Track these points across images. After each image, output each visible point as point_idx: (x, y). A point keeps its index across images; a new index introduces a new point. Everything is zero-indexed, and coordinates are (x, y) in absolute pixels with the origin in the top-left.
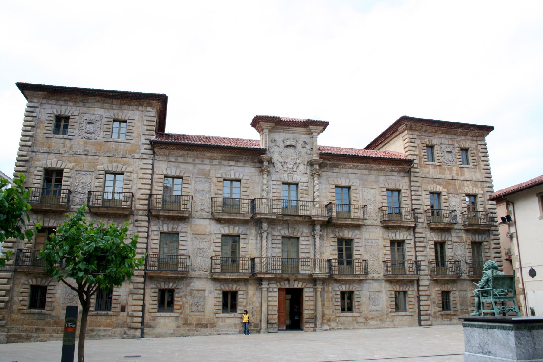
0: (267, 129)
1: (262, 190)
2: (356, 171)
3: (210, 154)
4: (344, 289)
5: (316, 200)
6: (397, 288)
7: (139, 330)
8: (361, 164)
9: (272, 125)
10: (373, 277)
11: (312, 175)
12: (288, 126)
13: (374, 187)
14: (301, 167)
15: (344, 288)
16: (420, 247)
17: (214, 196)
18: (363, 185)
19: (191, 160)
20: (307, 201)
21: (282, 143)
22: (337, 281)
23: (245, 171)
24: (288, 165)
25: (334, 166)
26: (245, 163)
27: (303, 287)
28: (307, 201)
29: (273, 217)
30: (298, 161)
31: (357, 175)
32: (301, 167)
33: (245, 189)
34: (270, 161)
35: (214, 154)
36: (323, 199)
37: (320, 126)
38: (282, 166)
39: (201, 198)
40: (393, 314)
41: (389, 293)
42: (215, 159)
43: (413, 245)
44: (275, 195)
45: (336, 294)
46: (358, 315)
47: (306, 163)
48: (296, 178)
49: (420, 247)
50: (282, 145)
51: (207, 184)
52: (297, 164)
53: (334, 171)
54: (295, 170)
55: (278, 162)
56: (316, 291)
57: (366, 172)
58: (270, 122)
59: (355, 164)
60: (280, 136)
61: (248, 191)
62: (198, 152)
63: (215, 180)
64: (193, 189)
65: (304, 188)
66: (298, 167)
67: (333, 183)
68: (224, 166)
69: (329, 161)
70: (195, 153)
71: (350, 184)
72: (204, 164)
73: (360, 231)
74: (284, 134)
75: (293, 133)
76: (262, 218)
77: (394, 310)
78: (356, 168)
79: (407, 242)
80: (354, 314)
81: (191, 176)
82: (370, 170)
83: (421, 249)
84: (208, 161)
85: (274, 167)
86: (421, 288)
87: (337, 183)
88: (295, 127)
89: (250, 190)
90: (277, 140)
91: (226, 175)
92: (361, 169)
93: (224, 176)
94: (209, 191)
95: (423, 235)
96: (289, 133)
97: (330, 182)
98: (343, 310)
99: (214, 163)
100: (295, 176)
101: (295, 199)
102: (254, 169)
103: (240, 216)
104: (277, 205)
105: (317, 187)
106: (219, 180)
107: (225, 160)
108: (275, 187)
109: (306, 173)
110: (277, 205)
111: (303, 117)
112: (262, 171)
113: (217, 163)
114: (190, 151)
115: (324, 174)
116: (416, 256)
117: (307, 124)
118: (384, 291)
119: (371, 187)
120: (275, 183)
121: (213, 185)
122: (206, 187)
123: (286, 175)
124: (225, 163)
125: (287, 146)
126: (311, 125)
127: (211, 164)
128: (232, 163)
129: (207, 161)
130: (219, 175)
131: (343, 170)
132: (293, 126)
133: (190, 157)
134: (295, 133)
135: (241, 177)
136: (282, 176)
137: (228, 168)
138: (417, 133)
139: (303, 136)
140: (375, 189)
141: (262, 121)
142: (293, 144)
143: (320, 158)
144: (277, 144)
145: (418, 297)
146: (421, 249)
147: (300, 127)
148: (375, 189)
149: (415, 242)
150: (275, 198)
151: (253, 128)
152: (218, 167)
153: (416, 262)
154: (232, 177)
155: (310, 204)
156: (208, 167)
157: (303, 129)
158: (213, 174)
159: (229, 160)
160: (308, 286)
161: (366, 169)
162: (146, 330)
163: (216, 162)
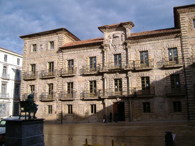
4: (144, 102)
6: (174, 100)
7: (61, 121)
10: (160, 95)
15: (144, 101)
16: (188, 77)
22: (140, 98)
27: (124, 101)
40: (172, 113)
41: (169, 102)
43: (183, 76)
45: (140, 104)
46: (152, 114)
49: (188, 77)
56: (129, 103)
73: (152, 71)
77: (173, 111)
79: (181, 75)
80: (150, 114)
83: (188, 78)
86: (189, 99)
95: (190, 70)
98: (145, 111)
116: (186, 82)
118: (166, 102)
138: (186, 14)
145: (188, 104)
146: (188, 78)
149: (185, 74)
153: (186, 85)
158: (84, 56)
160: (126, 101)
162: (63, 120)
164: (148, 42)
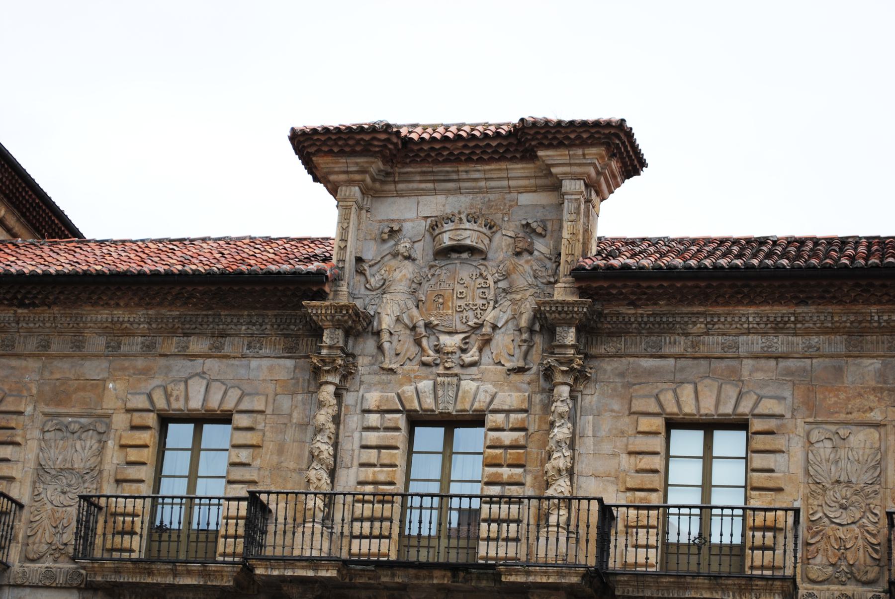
0: (350, 183)
1: (312, 457)
2: (780, 343)
3: (103, 315)
5: (550, 492)
8: (799, 310)
9: (376, 165)
11: (548, 373)
12: (447, 161)
13: (876, 416)
14: (503, 341)
17: (108, 489)
18: (811, 407)
19: (32, 345)
20: (510, 500)
21: (428, 237)
23: (258, 374)
24: (445, 340)
25: (661, 328)
26: (254, 342)
28: (510, 500)
29: (323, 573)
30: (490, 316)
31: (783, 364)
32: (503, 341)
33: (244, 455)
34: (358, 325)
35: (120, 314)
36: (590, 487)
37: (583, 144)
38: (418, 343)
39: (58, 499)
42: (130, 334)
44: (369, 474)
47: (523, 323)
48: (475, 391)
50: (422, 251)
51: (91, 442)
52: (487, 329)
53: (667, 350)
54: (468, 358)
55: (399, 327)
57: (838, 343)
58: (353, 153)
59: (767, 309)
60: (413, 210)
61: (257, 463)
62: (56, 310)
63: (120, 420)
64: (32, 465)
65: (507, 437)
66: (487, 342)
67: (654, 408)
68: (162, 361)
69: (633, 304)
70: (45, 313)
71: (745, 408)
72: (84, 357)
74: (441, 198)
75: (480, 191)
76: (283, 579)
78: (779, 327)
81: (29, 410)
82: (856, 334)
84: (102, 341)
85: (380, 348)
87: (671, 408)
88: (480, 161)
89: (268, 456)
90: (407, 226)
91: (168, 396)
92: (807, 333)
93: (161, 403)
94: (96, 472)
96: (459, 191)
97: (638, 405)
99: (124, 349)
100: (468, 385)
101: (435, 488)
102: (290, 363)
103: (189, 573)
104: (372, 519)
105: (561, 432)
106: (137, 419)
107: (173, 332)
108: (372, 438)
109: (520, 370)
110: (372, 519)
111: (500, 111)
112: (316, 372)
113: (137, 349)
114: (21, 305)
115: (609, 366)
117: (527, 141)
119: (856, 416)
120: (374, 419)
121: (110, 443)
122: (80, 452)
123: (425, 385)
124: (172, 345)
125: (445, 253)
126: (542, 146)
127: (113, 350)
128: (198, 345)
129: (97, 343)
130: (141, 402)
131: (713, 343)
132: (469, 160)
133: (30, 331)
134: (488, 190)
135: (229, 405)
136: (408, 390)
137: (182, 367)
139: (525, 199)
140: (877, 425)
141: (318, 151)
142: (469, 238)
143: (582, 292)
144: (401, 248)
147: (502, 158)
148: (877, 425)
150: (369, 489)
151: (320, 187)
152: (140, 363)
154: (195, 404)
155: (529, 512)
156: (93, 369)
157: (519, 169)
159: (186, 335)
161: (834, 331)
163: (134, 344)
164: (757, 343)
